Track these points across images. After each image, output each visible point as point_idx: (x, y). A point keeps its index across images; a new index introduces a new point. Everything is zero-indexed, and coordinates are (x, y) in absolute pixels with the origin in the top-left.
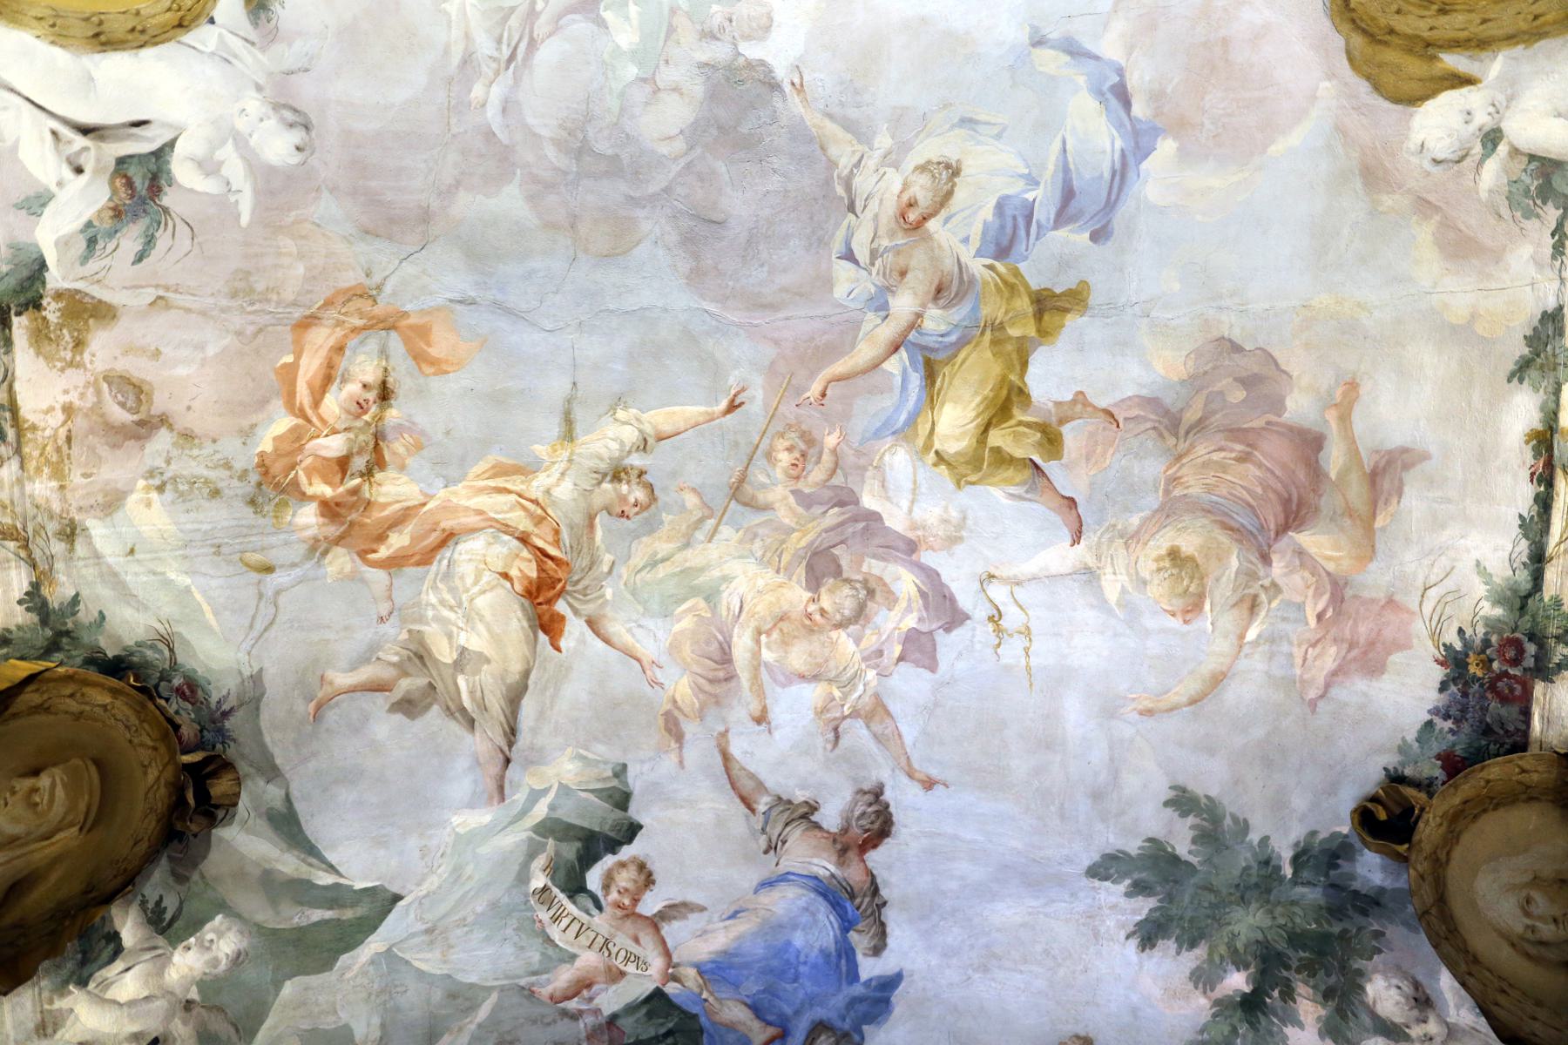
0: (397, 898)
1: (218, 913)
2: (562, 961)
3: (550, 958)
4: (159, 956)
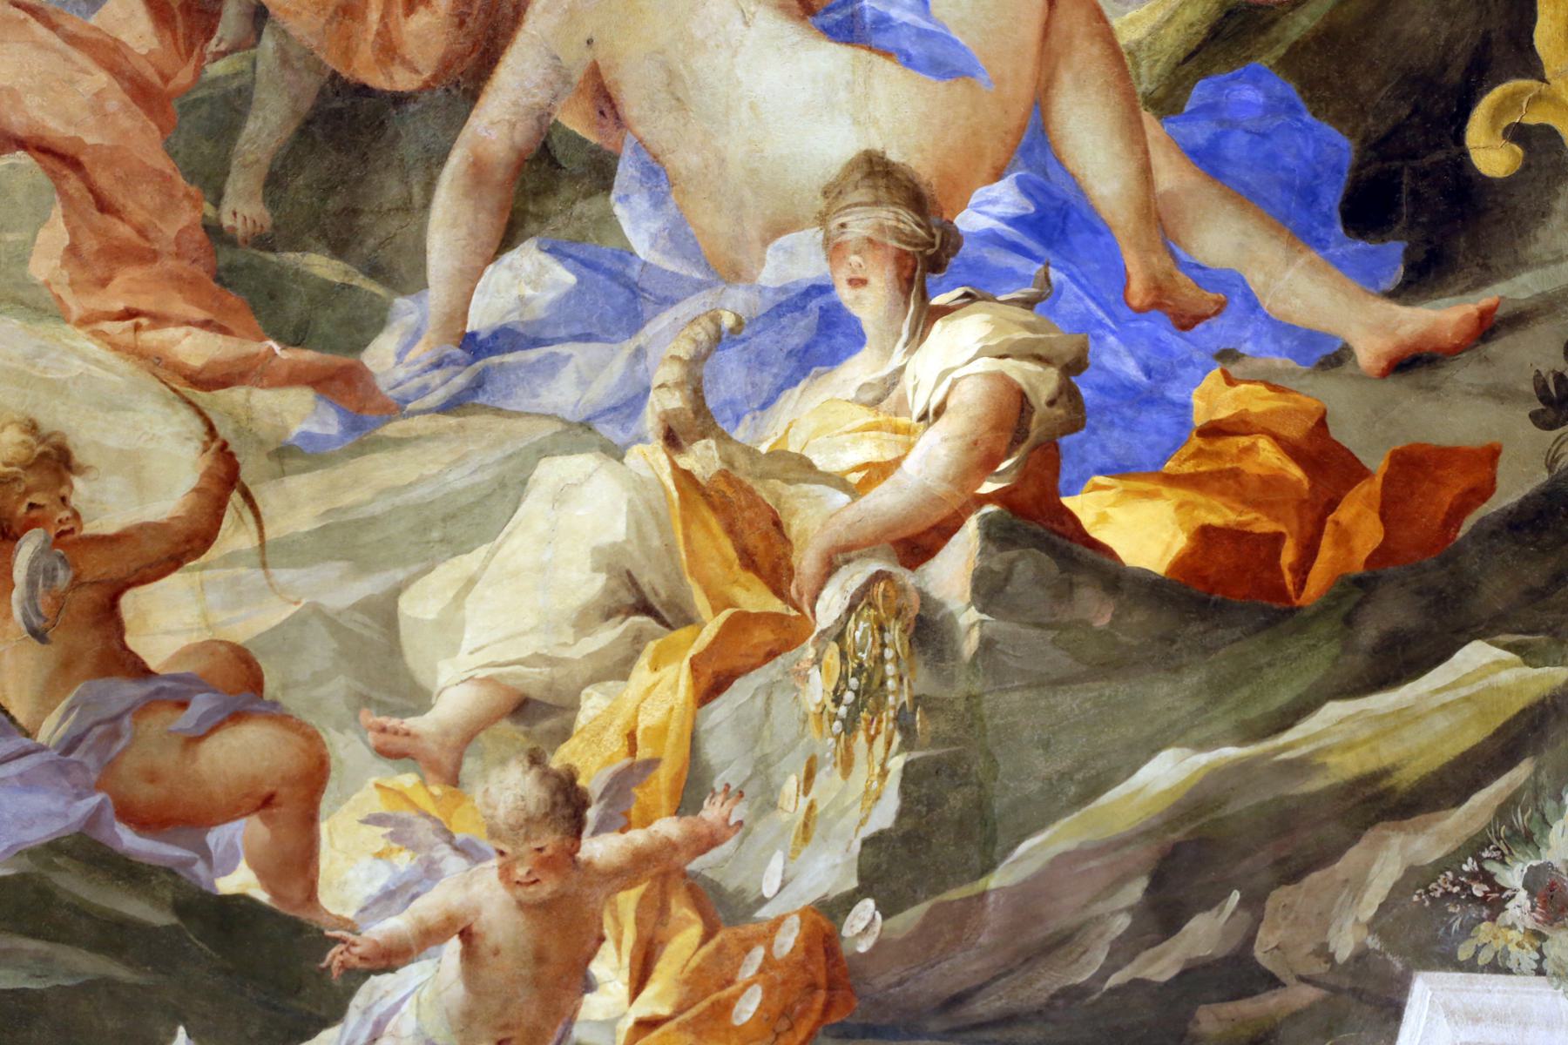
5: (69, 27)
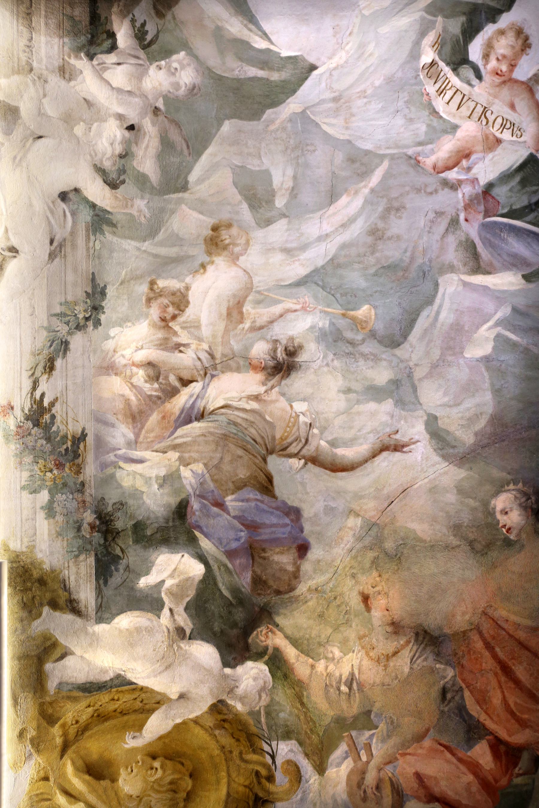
0: (313, 68)
1: (183, 50)
2: (445, 132)
3: (434, 128)
4: (141, 65)
5: (460, 755)
